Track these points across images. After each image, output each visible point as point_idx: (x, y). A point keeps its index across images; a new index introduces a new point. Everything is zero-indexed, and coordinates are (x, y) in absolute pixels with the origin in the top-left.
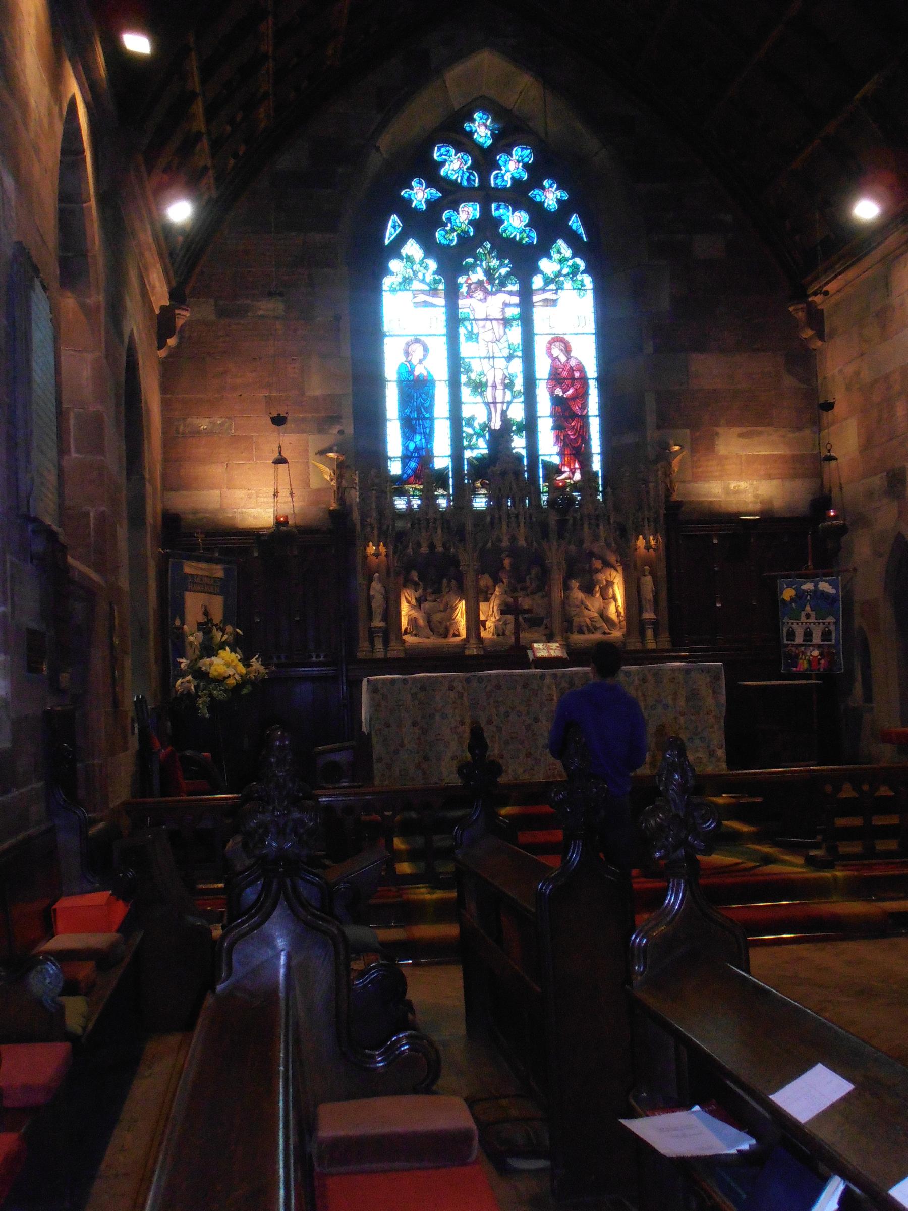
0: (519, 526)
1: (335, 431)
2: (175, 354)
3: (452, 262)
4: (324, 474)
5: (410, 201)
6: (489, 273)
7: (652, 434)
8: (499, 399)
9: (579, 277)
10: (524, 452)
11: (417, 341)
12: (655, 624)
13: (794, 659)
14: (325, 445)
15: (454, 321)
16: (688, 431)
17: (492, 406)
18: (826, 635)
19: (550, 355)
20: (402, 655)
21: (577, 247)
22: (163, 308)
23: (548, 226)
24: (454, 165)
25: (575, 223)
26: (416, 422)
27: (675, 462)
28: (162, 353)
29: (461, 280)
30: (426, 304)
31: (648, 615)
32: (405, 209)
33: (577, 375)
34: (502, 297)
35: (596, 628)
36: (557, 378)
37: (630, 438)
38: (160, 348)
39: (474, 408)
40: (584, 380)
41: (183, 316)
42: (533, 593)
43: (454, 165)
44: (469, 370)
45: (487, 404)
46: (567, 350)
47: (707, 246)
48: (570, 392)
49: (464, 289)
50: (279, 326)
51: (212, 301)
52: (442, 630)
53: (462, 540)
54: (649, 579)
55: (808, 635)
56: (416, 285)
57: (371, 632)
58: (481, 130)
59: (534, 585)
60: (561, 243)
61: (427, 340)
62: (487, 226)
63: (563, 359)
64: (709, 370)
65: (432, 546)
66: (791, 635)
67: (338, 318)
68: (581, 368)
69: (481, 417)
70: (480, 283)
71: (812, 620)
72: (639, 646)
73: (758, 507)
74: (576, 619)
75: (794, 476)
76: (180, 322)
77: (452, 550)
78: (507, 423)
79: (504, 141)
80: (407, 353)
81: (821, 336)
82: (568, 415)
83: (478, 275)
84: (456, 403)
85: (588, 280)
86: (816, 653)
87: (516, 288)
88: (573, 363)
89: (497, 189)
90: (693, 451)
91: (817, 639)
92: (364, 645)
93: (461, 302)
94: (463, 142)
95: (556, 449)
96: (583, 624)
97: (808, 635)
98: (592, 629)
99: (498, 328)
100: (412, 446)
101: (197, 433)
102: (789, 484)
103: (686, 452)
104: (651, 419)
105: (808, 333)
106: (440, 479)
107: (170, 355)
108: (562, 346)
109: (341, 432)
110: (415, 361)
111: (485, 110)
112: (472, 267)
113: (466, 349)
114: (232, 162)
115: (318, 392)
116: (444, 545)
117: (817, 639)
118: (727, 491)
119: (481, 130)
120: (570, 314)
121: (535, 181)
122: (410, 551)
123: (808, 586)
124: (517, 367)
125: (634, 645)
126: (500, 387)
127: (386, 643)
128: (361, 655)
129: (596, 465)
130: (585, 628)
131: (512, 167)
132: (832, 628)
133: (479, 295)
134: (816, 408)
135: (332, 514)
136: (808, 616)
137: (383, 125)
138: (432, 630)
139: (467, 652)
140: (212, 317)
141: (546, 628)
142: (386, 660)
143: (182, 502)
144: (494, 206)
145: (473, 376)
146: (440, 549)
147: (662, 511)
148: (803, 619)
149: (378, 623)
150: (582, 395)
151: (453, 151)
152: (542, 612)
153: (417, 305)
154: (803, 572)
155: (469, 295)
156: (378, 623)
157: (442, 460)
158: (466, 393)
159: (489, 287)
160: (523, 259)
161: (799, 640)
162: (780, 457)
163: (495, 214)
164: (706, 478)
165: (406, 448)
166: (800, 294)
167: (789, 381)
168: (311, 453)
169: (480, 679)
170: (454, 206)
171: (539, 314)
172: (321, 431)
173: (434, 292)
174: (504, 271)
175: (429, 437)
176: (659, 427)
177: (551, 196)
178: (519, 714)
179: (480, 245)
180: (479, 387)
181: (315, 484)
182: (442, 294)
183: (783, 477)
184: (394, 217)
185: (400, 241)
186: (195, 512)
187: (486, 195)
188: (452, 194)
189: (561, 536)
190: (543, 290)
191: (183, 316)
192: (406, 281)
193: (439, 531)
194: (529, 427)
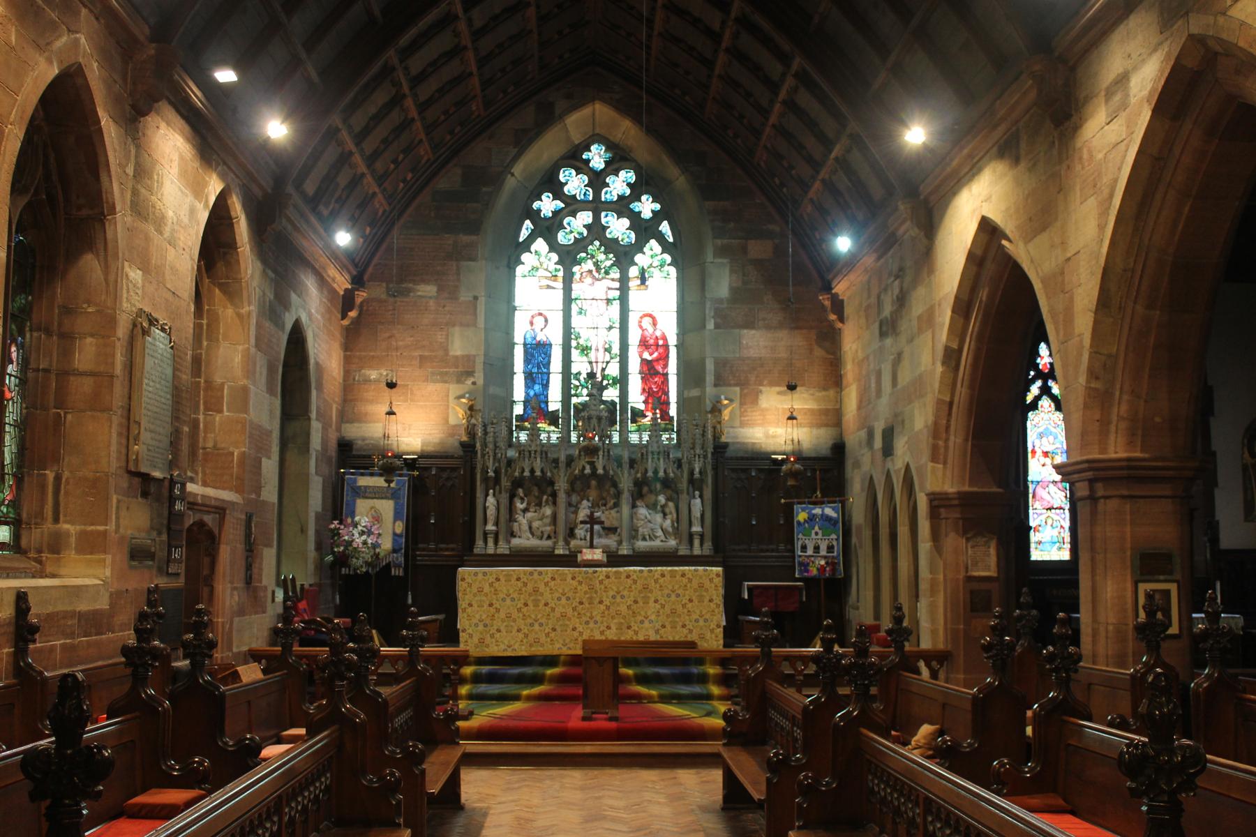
1: (469, 382)
2: (357, 322)
3: (568, 257)
4: (458, 415)
5: (539, 211)
6: (596, 264)
7: (710, 390)
8: (600, 360)
9: (666, 268)
10: (617, 400)
11: (540, 314)
12: (702, 536)
13: (805, 566)
14: (459, 393)
15: (568, 300)
16: (738, 389)
18: (830, 548)
19: (641, 327)
20: (507, 552)
21: (666, 247)
22: (346, 290)
23: (644, 230)
24: (574, 183)
25: (665, 227)
26: (537, 376)
27: (726, 414)
28: (346, 322)
29: (576, 269)
30: (549, 287)
31: (696, 528)
32: (535, 216)
33: (661, 342)
36: (644, 344)
37: (695, 393)
38: (343, 318)
39: (580, 365)
40: (666, 347)
41: (361, 296)
43: (574, 183)
46: (655, 324)
47: (758, 249)
48: (656, 355)
49: (577, 277)
50: (432, 303)
51: (384, 285)
52: (539, 533)
53: (557, 467)
54: (698, 501)
55: (817, 549)
56: (541, 272)
57: (485, 534)
58: (597, 157)
60: (653, 243)
62: (596, 229)
63: (651, 330)
64: (755, 343)
65: (532, 471)
66: (804, 548)
67: (476, 298)
68: (664, 338)
70: (590, 271)
71: (820, 536)
72: (687, 552)
73: (789, 448)
75: (819, 426)
76: (358, 300)
79: (613, 167)
80: (532, 323)
81: (841, 319)
82: (651, 371)
83: (589, 265)
85: (673, 271)
86: (823, 562)
87: (617, 276)
88: (658, 334)
89: (606, 202)
90: (742, 404)
91: (823, 552)
92: (479, 543)
93: (574, 286)
94: (583, 168)
95: (643, 398)
97: (817, 549)
98: (652, 537)
99: (603, 304)
100: (532, 393)
101: (367, 381)
102: (815, 431)
103: (736, 405)
104: (710, 378)
105: (833, 317)
106: (553, 419)
107: (352, 323)
108: (648, 319)
109: (474, 383)
111: (599, 142)
112: (585, 259)
113: (576, 321)
114: (402, 185)
115: (459, 353)
116: (542, 471)
117: (823, 552)
118: (767, 436)
119: (597, 157)
120: (659, 295)
121: (636, 195)
123: (817, 511)
124: (615, 334)
125: (683, 551)
126: (601, 350)
127: (496, 542)
128: (476, 551)
129: (673, 411)
131: (618, 185)
132: (835, 543)
133: (589, 280)
134: (834, 379)
135: (463, 444)
136: (817, 534)
137: (516, 159)
138: (533, 534)
139: (557, 552)
140: (384, 296)
142: (495, 555)
143: (353, 431)
144: (603, 214)
145: (582, 341)
146: (538, 473)
147: (710, 450)
148: (813, 536)
149: (490, 527)
150: (664, 358)
151: (574, 172)
152: (616, 524)
153: (541, 287)
154: (814, 499)
156: (490, 527)
157: (555, 404)
158: (575, 354)
159: (596, 275)
160: (623, 255)
161: (810, 552)
162: (809, 410)
163: (603, 221)
164: (753, 425)
165: (527, 394)
166: (827, 288)
167: (819, 352)
168: (451, 398)
169: (540, 573)
170: (574, 214)
171: (635, 296)
172: (459, 381)
174: (608, 263)
175: (546, 386)
176: (716, 385)
177: (646, 207)
178: (568, 599)
180: (585, 350)
181: (452, 421)
182: (561, 279)
183: (811, 426)
184: (528, 223)
186: (364, 439)
187: (597, 206)
188: (572, 205)
189: (631, 466)
191: (361, 296)
192: (535, 269)
194: (622, 381)
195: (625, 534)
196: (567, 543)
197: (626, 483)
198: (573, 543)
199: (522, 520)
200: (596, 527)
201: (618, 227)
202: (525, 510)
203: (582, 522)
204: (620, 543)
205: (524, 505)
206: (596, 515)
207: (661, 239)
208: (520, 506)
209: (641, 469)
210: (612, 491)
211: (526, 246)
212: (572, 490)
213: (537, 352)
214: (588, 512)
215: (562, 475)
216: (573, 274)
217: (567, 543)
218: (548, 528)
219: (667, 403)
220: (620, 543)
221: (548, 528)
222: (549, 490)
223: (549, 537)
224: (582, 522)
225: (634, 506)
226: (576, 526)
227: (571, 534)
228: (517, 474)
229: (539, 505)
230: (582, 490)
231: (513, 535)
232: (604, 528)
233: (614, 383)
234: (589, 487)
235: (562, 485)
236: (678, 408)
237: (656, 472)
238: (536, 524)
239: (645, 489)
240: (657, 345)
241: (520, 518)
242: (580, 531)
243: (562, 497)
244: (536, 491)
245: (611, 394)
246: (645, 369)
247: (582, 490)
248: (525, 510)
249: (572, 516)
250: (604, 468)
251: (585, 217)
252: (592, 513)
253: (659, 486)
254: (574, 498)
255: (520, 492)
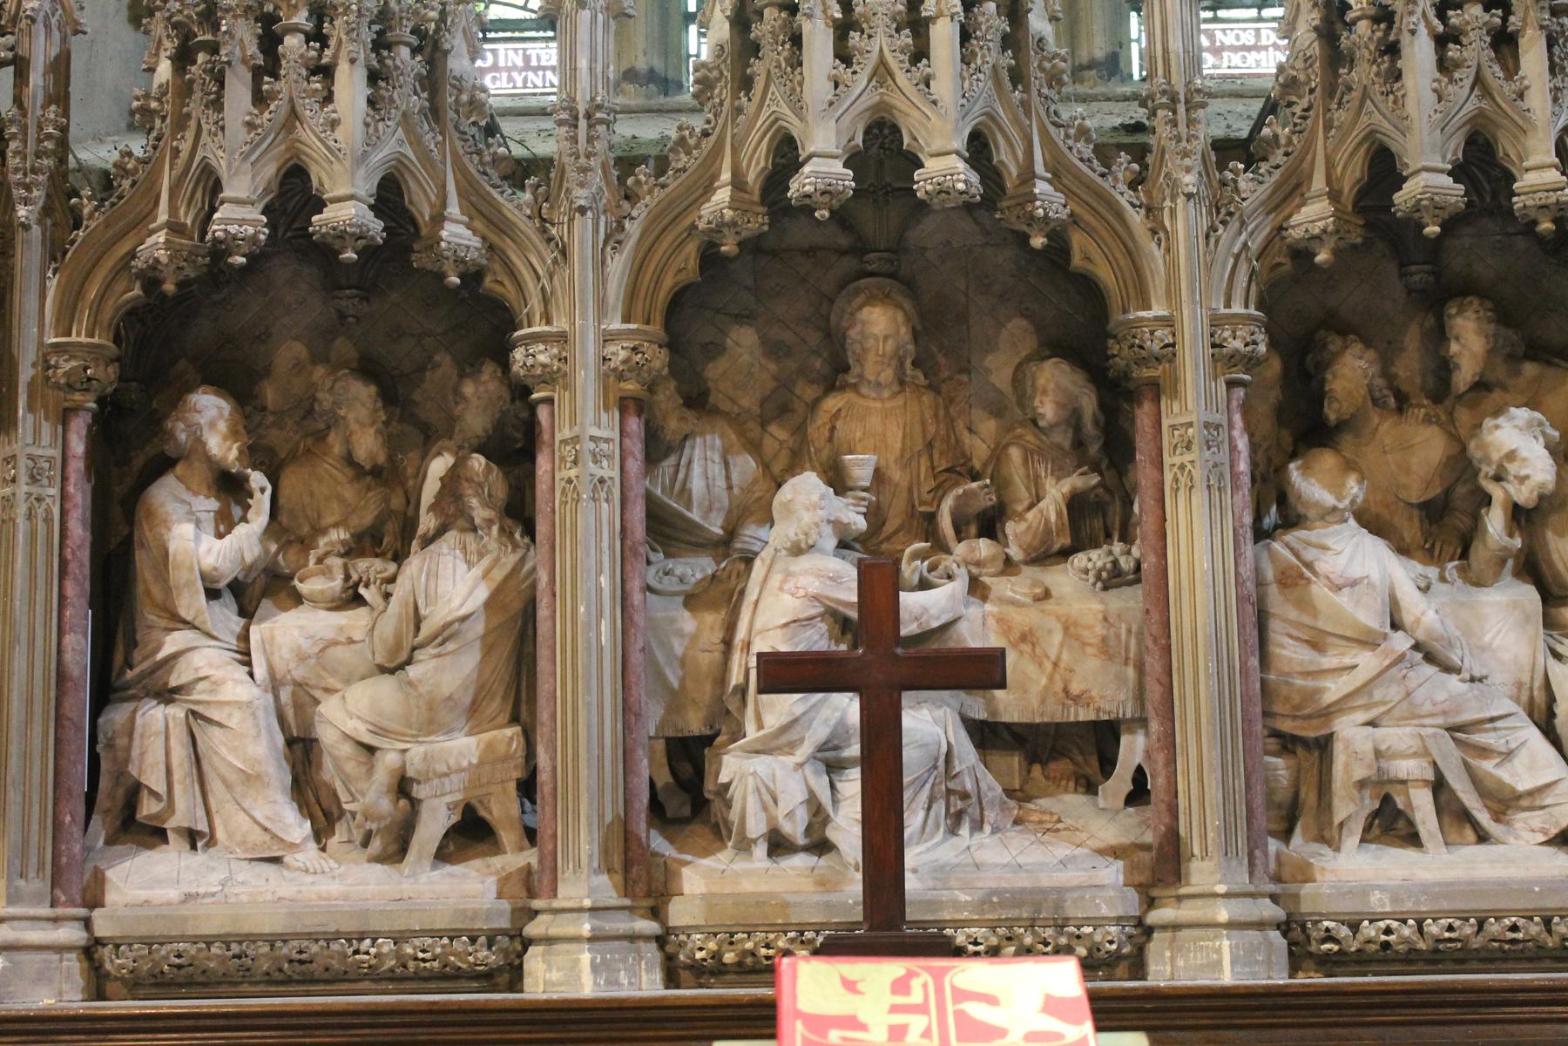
0: (920, 53)
35: (1505, 803)
42: (1047, 555)
52: (369, 796)
59: (1056, 493)
74: (1350, 733)
77: (458, 234)
96: (1406, 768)
116: (389, 197)
122: (156, 245)
130: (1422, 806)
138: (322, 812)
141: (1139, 794)
152: (1102, 690)
193: (350, 87)
195: (1204, 787)
196: (647, 887)
197: (1191, 294)
198: (706, 883)
199: (220, 683)
200: (928, 723)
202: (255, 591)
203: (784, 673)
204: (1161, 867)
205: (245, 542)
206: (921, 607)
208: (196, 540)
209: (1335, 162)
210: (1056, 388)
212: (673, 393)
214: (841, 581)
215: (583, 235)
217: (647, 887)
218: (463, 747)
220: (1161, 867)
221: (463, 747)
222: (477, 404)
223: (471, 833)
224: (784, 673)
225: (1275, 511)
226: (724, 722)
227: (683, 793)
228: (156, 245)
229: (390, 538)
230: (778, 407)
231: (138, 829)
232: (986, 735)
234: (837, 372)
235: (582, 323)
237: (1482, 162)
238: (342, 717)
239: (1351, 373)
241: (201, 656)
242: (777, 764)
243: (585, 440)
244: (360, 424)
247: (778, 407)
248: (255, 591)
249: (692, 629)
250: (978, 149)
252: (880, 583)
253: (1470, 340)
254: (708, 472)
255: (210, 420)
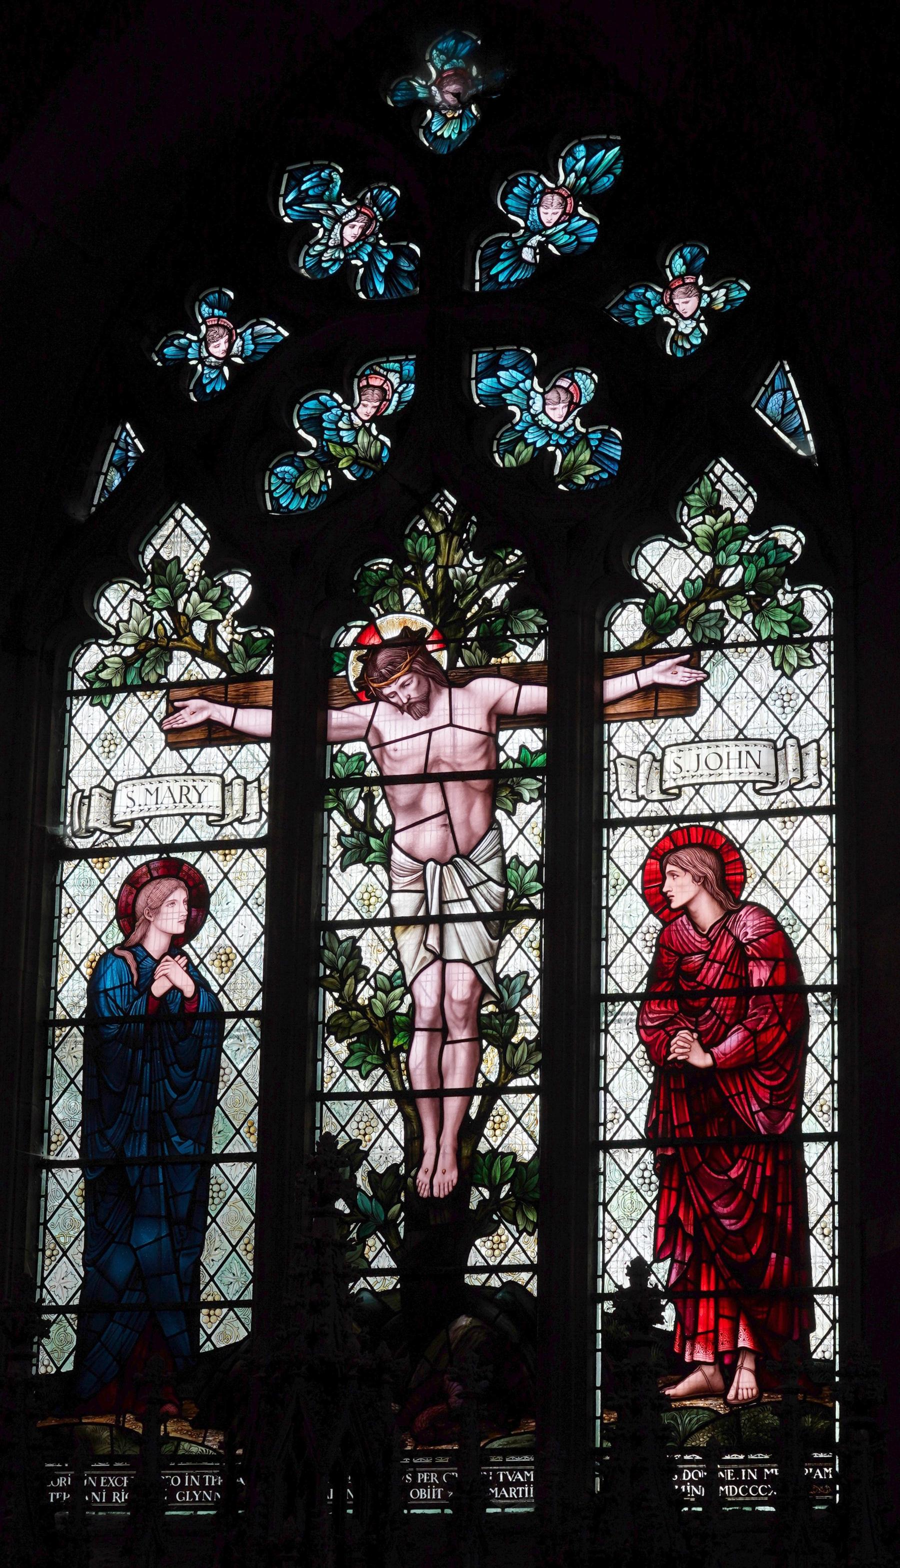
6: (443, 604)
8: (456, 1080)
15: (304, 783)
17: (425, 1105)
19: (656, 900)
21: (781, 488)
30: (215, 734)
34: (491, 689)
36: (674, 987)
44: (352, 966)
45: (406, 1098)
56: (180, 666)
58: (443, 100)
61: (207, 866)
62: (446, 437)
63: (707, 912)
68: (779, 947)
69: (386, 1151)
78: (472, 1165)
84: (289, 1090)
88: (748, 927)
100: (120, 1266)
108: (705, 862)
110: (155, 944)
113: (348, 890)
129: (823, 1341)
133: (406, 687)
153: (177, 739)
155: (368, 692)
173: (235, 688)
179: (422, 504)
180: (380, 1036)
185: (140, 510)
188: (333, 334)
190: (644, 653)
192: (154, 649)
194: (561, 1189)
201: (546, 410)
207: (761, 459)
211: (119, 558)
213: (154, 1042)
216: (328, 660)
219: (803, 1295)
233: (520, 1199)
236: (844, 1322)
240: (743, 989)
245: (506, 1253)
246: (681, 1115)
251: (390, 385)
